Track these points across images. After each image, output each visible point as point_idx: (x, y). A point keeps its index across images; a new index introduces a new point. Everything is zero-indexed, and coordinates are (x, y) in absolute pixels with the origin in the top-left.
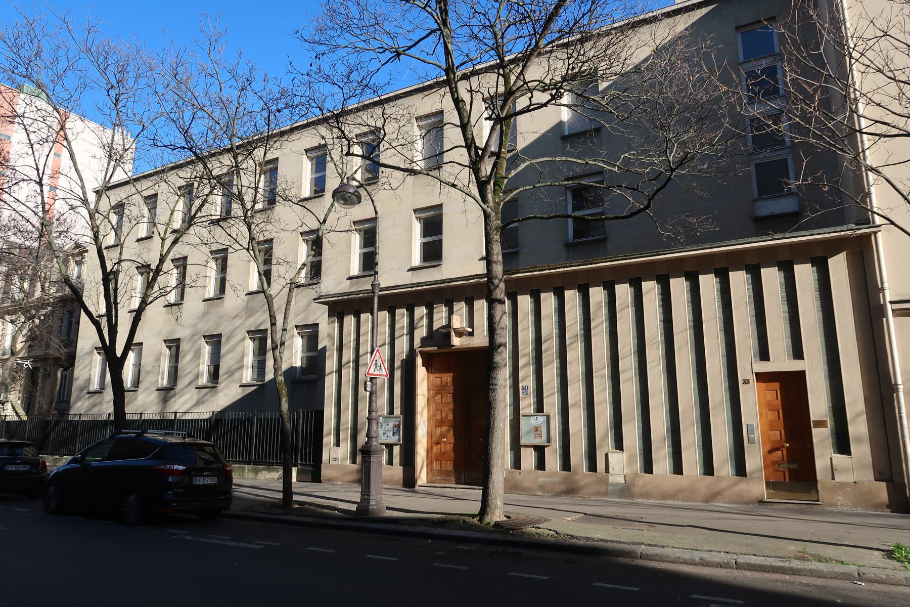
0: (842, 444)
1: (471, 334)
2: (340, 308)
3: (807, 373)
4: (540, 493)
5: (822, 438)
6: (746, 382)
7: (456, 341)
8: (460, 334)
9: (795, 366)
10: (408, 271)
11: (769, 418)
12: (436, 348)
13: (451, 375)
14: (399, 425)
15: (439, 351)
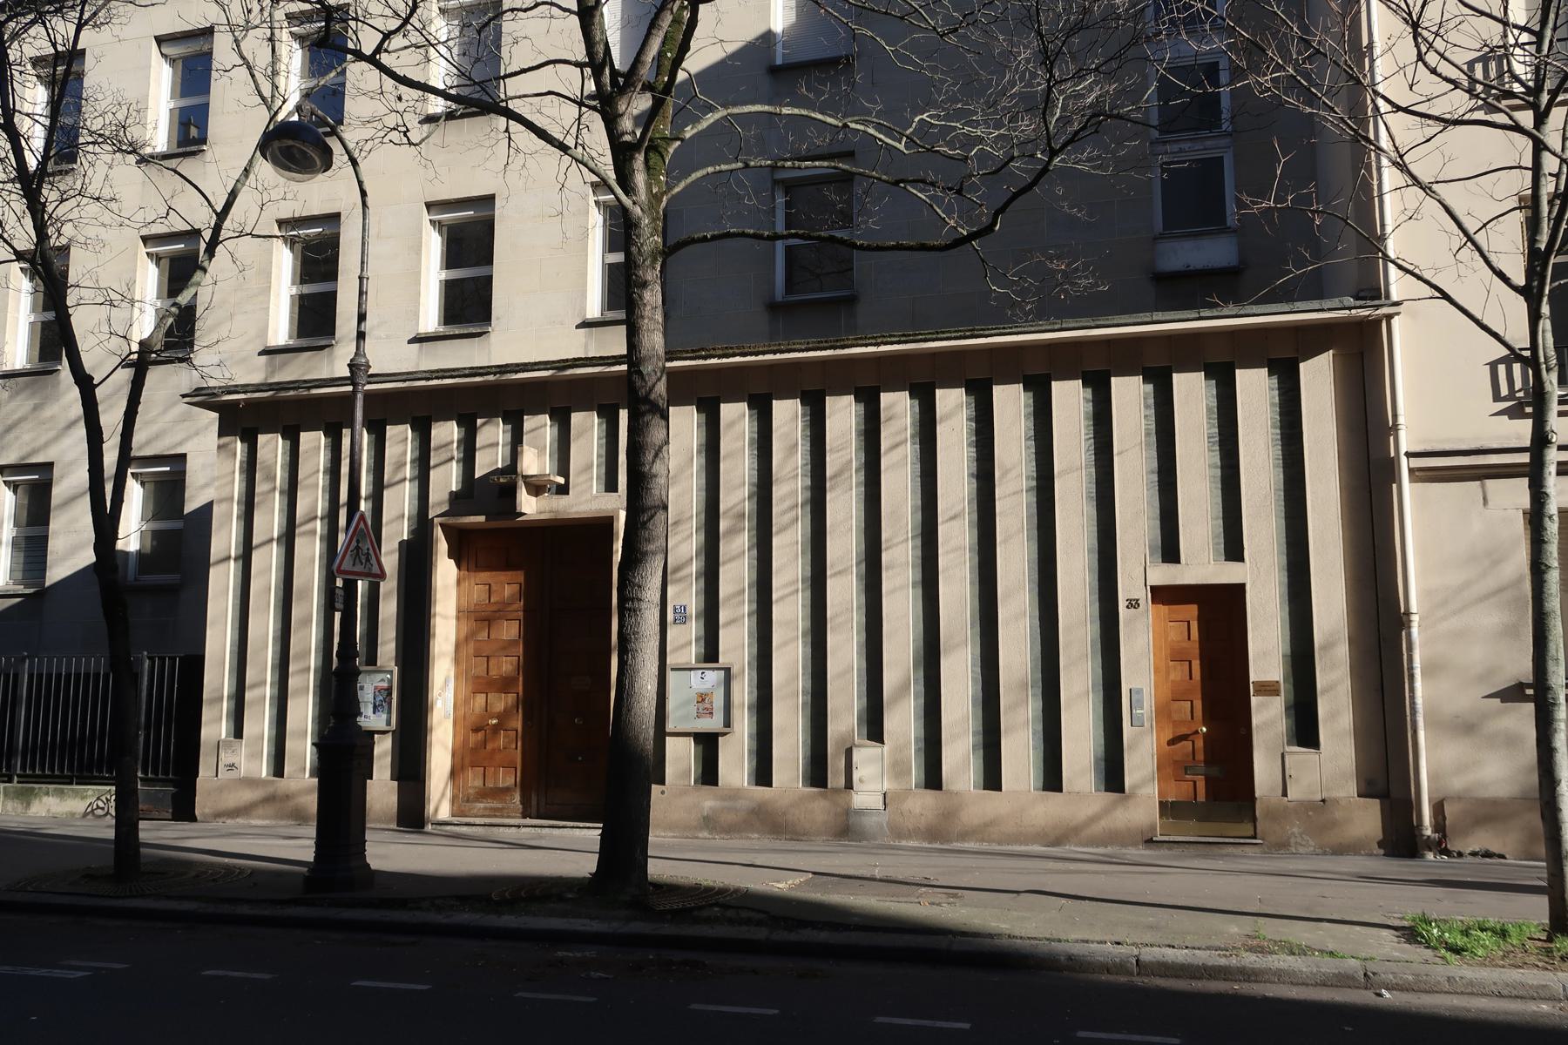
0: (1305, 730)
1: (563, 490)
2: (243, 417)
3: (1248, 588)
4: (705, 834)
5: (1268, 717)
6: (1133, 604)
7: (529, 506)
8: (537, 488)
9: (1228, 573)
10: (410, 342)
11: (1172, 677)
12: (482, 519)
13: (520, 576)
14: (389, 690)
15: (487, 524)
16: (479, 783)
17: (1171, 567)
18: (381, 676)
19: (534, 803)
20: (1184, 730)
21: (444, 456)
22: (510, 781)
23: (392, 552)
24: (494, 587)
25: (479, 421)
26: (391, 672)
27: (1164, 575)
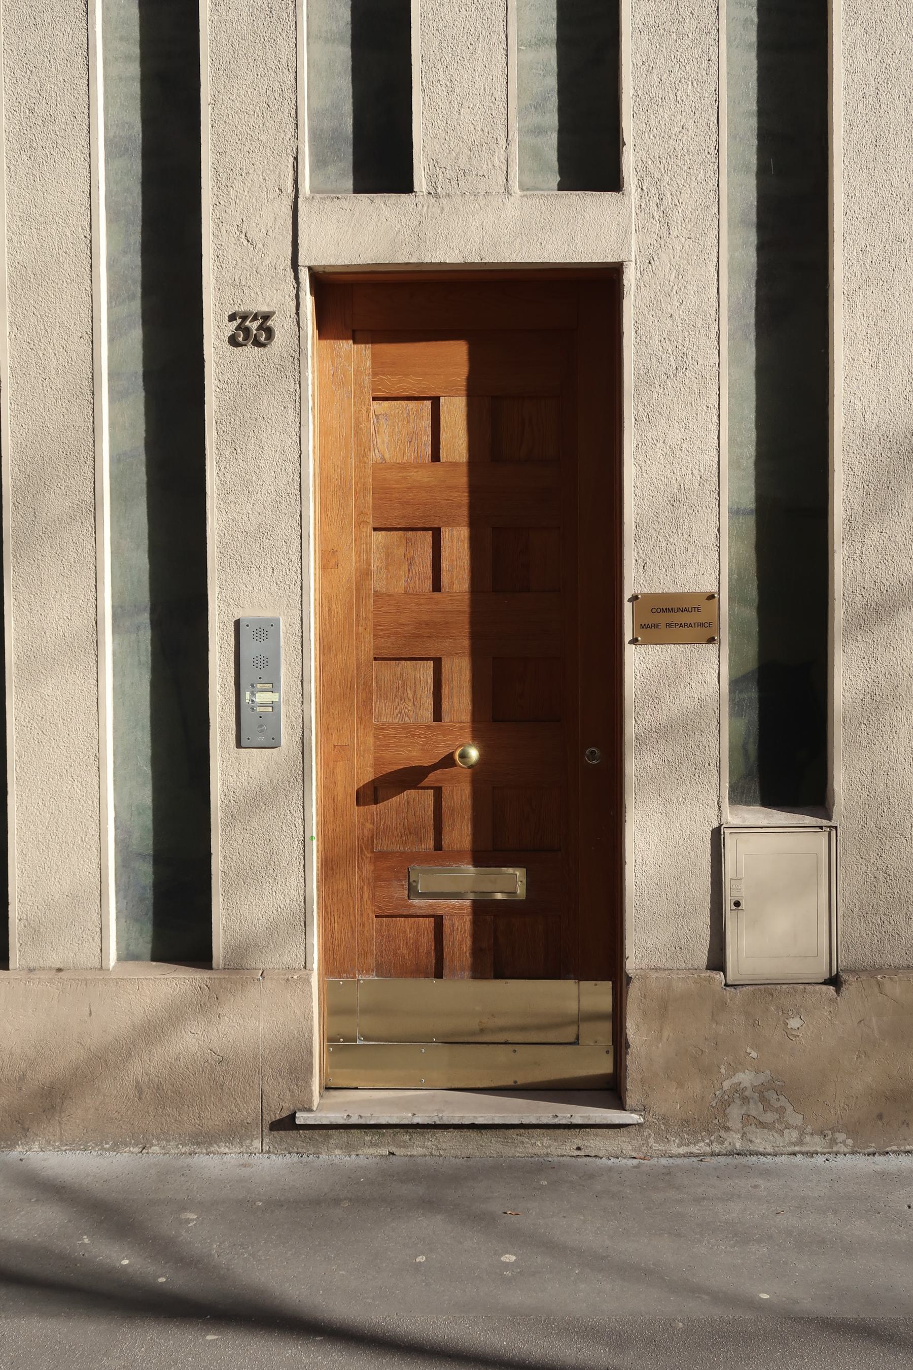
3: (630, 278)
6: (252, 330)
17: (384, 208)
20: (412, 755)
27: (365, 233)
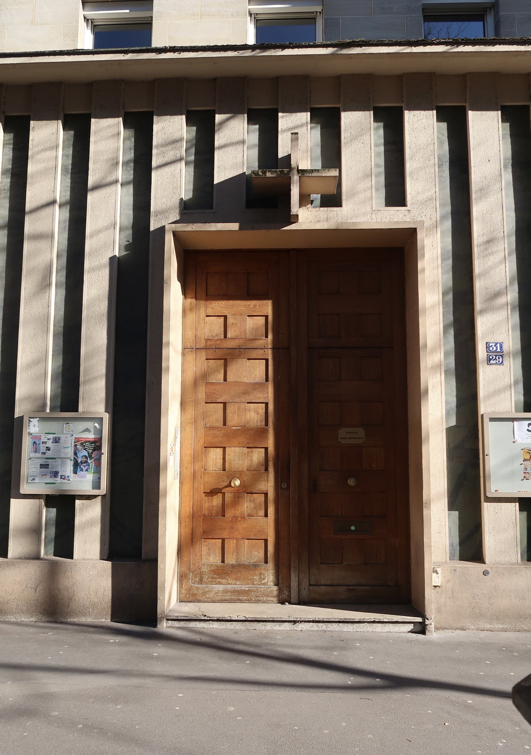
12: (235, 226)
13: (267, 307)
14: (97, 445)
16: (215, 559)
18: (89, 425)
19: (294, 584)
21: (170, 155)
22: (258, 555)
23: (99, 268)
24: (230, 321)
25: (219, 118)
26: (100, 420)
